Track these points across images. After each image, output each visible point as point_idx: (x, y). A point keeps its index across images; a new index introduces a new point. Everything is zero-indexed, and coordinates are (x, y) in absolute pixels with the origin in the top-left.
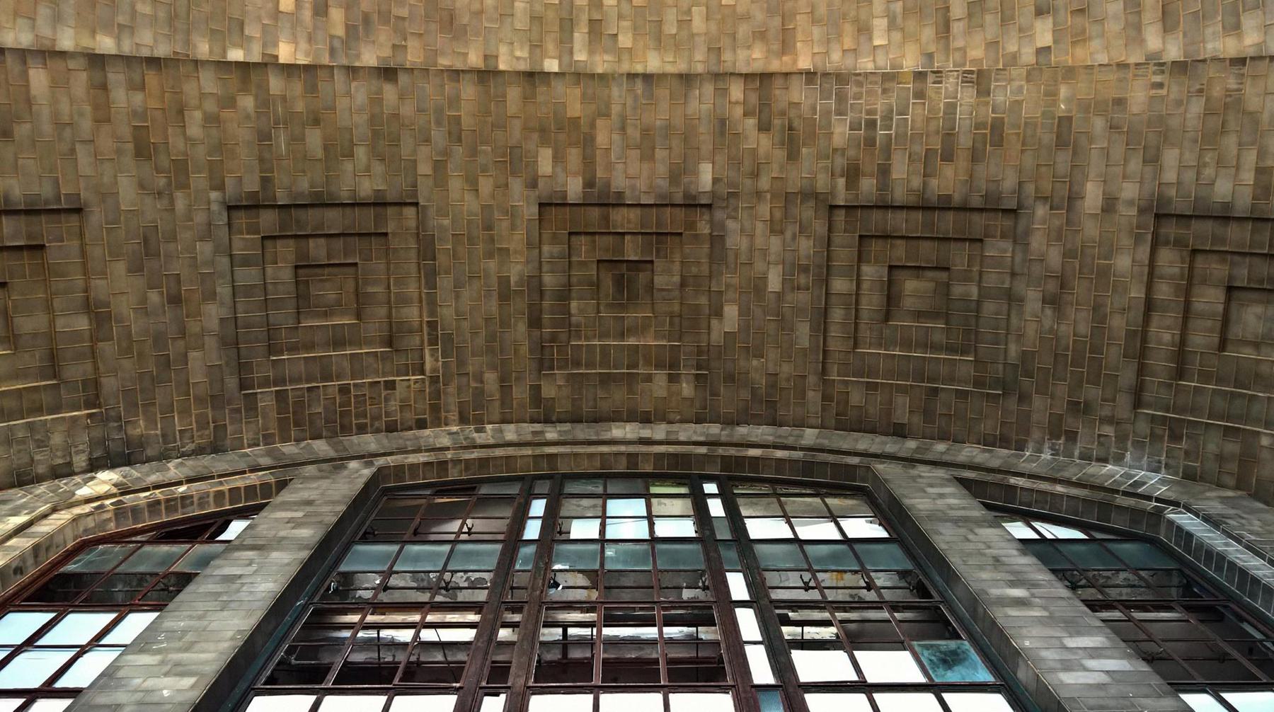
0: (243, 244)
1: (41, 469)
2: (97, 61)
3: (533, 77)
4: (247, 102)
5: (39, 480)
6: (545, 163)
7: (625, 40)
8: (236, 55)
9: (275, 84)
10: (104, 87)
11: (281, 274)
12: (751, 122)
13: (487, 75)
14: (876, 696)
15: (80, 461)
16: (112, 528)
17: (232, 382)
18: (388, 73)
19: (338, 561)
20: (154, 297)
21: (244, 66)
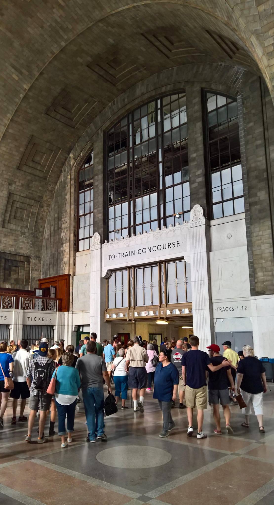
0: (53, 114)
1: (64, 161)
2: (12, 120)
3: (62, 50)
4: (31, 100)
5: (65, 162)
6: (80, 60)
7: (70, 27)
8: (22, 96)
9: (30, 94)
10: (16, 122)
11: (62, 111)
12: (109, 28)
13: (55, 58)
14: (166, 186)
15: (67, 155)
16: (79, 167)
17: (72, 129)
18: (41, 74)
19: (108, 169)
20: (52, 133)
21: (25, 97)
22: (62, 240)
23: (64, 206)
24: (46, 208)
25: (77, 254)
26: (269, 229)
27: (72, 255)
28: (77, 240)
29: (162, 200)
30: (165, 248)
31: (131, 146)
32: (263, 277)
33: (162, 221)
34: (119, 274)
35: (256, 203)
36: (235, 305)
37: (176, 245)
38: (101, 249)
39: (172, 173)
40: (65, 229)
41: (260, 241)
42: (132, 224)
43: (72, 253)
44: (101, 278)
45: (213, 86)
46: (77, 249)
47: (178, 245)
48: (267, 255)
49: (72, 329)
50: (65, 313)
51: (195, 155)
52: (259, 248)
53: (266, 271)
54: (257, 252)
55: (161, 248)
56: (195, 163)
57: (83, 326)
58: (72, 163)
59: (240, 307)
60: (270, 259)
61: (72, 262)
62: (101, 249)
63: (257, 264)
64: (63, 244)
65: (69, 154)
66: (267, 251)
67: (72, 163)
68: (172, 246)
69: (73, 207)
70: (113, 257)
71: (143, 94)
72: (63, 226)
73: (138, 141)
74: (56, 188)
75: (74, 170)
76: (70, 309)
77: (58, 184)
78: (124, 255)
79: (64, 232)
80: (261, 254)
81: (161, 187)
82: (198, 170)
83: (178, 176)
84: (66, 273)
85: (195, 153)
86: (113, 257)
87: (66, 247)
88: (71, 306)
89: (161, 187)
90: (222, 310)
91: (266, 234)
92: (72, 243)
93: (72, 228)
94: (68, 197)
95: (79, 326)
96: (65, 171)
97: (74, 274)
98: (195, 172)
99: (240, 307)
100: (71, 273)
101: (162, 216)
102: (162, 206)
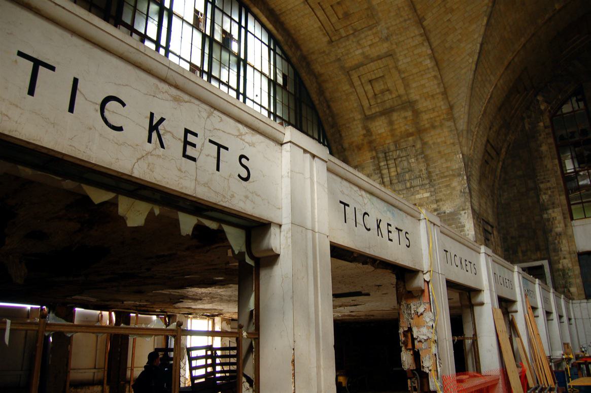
40: (547, 189)
64: (547, 209)
67: (542, 107)
72: (542, 186)
79: (545, 194)
94: (544, 148)
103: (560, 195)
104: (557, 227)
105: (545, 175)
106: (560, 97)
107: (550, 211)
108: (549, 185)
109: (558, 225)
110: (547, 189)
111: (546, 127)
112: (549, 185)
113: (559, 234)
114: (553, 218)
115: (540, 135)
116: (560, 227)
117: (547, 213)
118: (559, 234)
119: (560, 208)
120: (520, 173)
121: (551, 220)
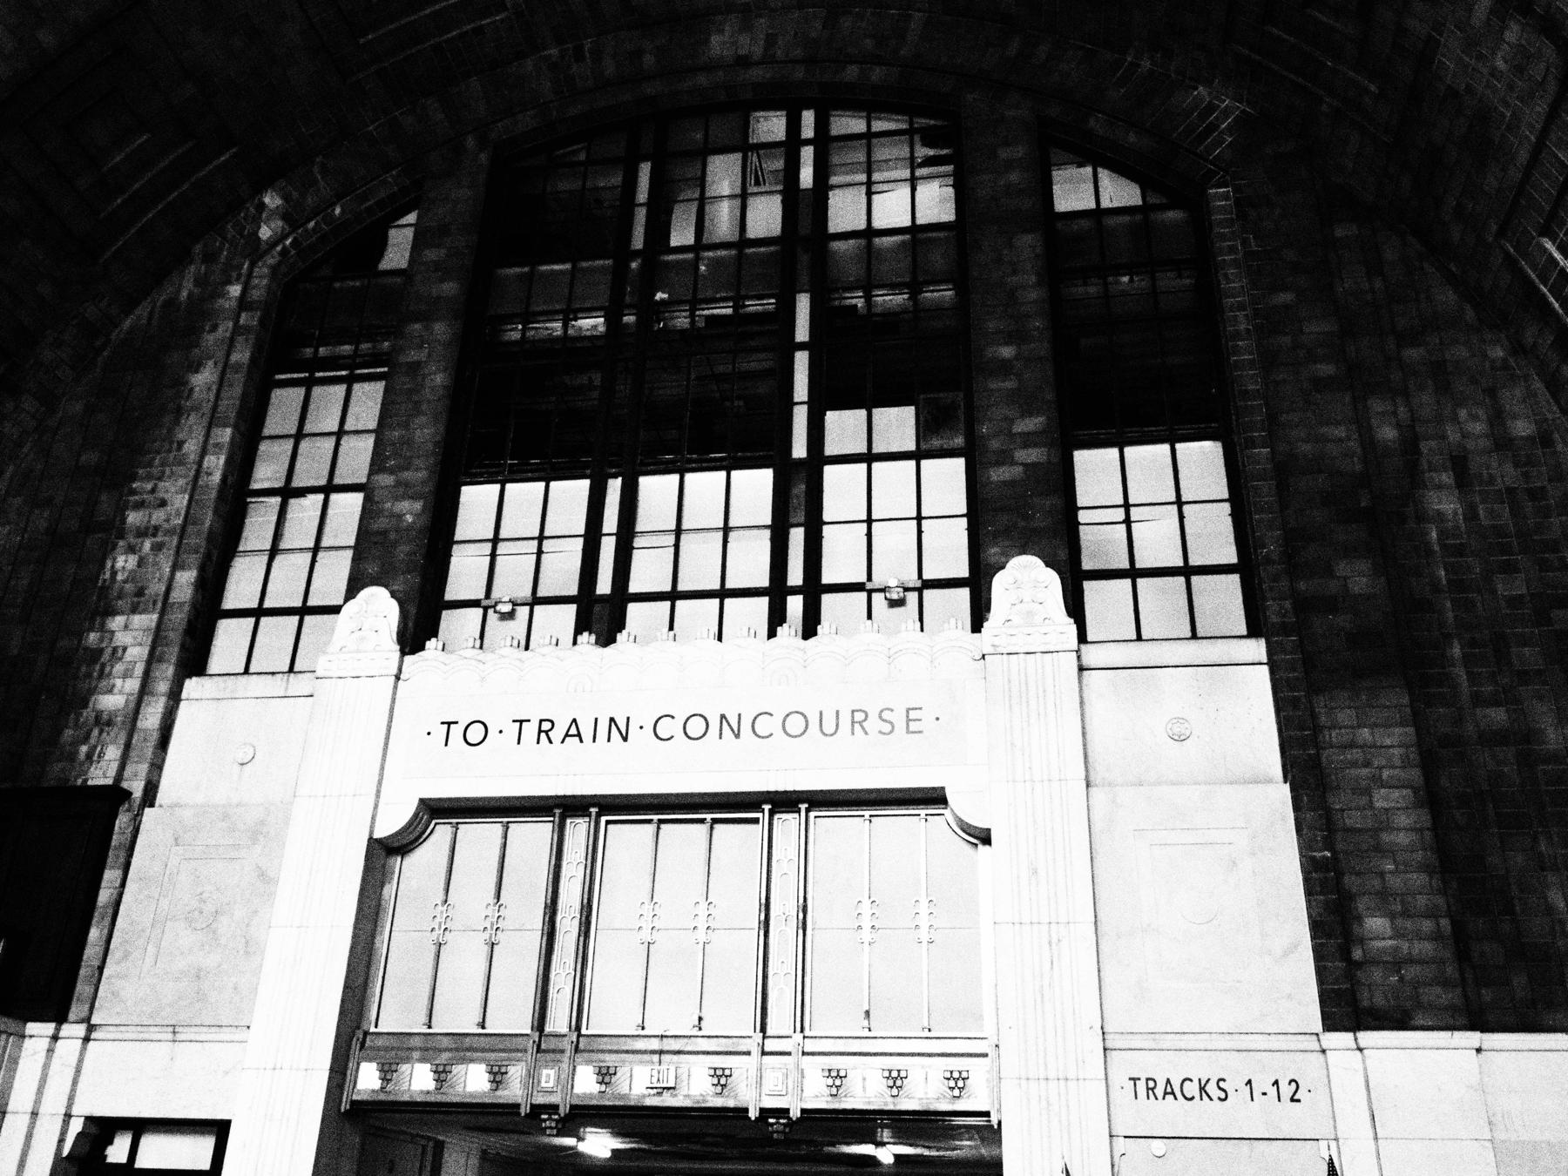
22: (105, 590)
23: (167, 419)
24: (29, 404)
25: (192, 686)
26: (1402, 725)
27: (163, 687)
28: (208, 609)
29: (798, 503)
30: (829, 728)
31: (638, 242)
32: (1390, 942)
33: (795, 604)
34: (480, 836)
35: (1331, 604)
36: (1235, 1071)
37: (900, 724)
38: (398, 678)
39: (868, 398)
40: (142, 533)
41: (1365, 771)
42: (604, 586)
43: (169, 670)
44: (371, 839)
45: (1096, 124)
46: (195, 662)
47: (913, 726)
48: (1403, 839)
49: (61, 1141)
50: (32, 1028)
51: (1007, 352)
52: (1364, 801)
53: (1406, 914)
54: (1354, 819)
55: (796, 723)
56: (1009, 384)
57: (139, 1127)
58: (265, 233)
59: (1263, 1083)
60: (1419, 856)
61: (151, 718)
62: (398, 678)
63: (1358, 874)
65: (260, 190)
66: (1403, 820)
67: (265, 233)
68: (873, 724)
69: (225, 435)
70: (475, 733)
71: (743, 62)
72: (133, 518)
73: (682, 235)
74: (127, 323)
75: (274, 269)
76: (76, 1011)
77: (142, 311)
78: (557, 735)
79: (131, 549)
80: (1376, 831)
81: (799, 450)
82: (1027, 413)
83: (897, 425)
84: (101, 775)
85: (1007, 344)
86: (475, 733)
87: (131, 634)
88: (82, 988)
89: (799, 450)
90: (1159, 1091)
91: (1388, 742)
92: (179, 618)
93: (196, 540)
94: (203, 379)
95: (102, 1129)
96: (210, 258)
97: (150, 797)
98: (1012, 421)
99: (1263, 1083)
100: (137, 788)
101: (795, 576)
102: (797, 536)
103: (175, 567)
104: (110, 691)
105: (160, 479)
106: (338, 211)
107: (117, 622)
108: (158, 516)
109: (119, 682)
110: (142, 533)
111: (243, 303)
112: (158, 516)
113: (105, 717)
114: (115, 650)
115: (214, 328)
116: (121, 693)
117: (103, 625)
118: (105, 717)
119: (155, 617)
120: (90, 458)
121: (106, 656)
